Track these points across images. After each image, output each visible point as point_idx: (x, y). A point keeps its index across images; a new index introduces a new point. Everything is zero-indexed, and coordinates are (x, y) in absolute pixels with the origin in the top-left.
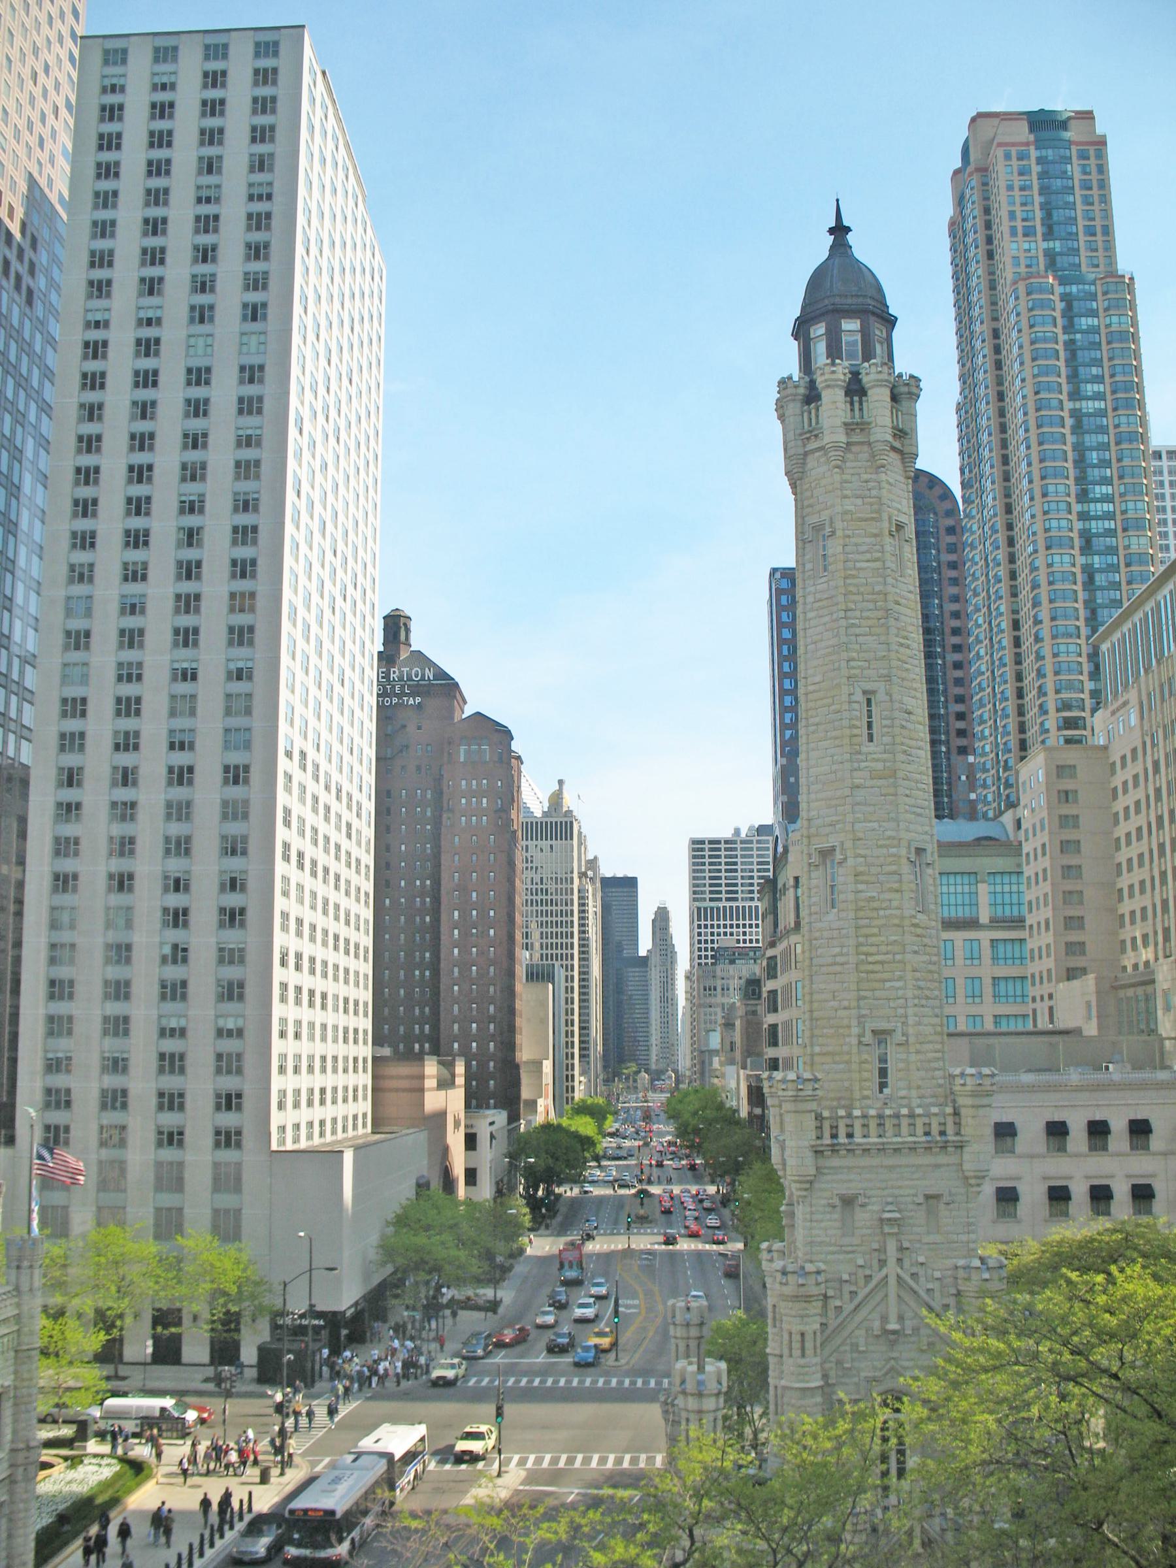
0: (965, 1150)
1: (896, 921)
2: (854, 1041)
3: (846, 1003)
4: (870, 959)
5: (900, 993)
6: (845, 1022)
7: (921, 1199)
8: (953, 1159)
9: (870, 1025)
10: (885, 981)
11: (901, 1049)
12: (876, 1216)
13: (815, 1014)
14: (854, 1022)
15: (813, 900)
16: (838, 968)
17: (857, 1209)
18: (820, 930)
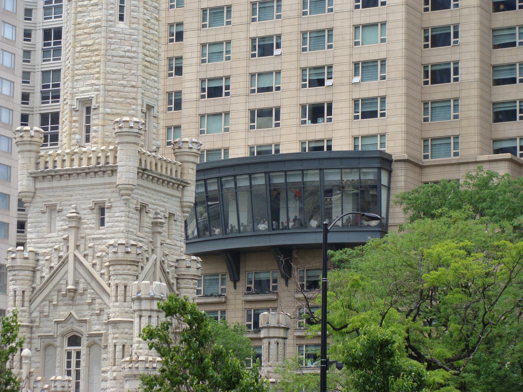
0: (186, 188)
1: (156, 39)
2: (139, 108)
3: (134, 83)
4: (147, 59)
5: (156, 84)
6: (133, 95)
7: (167, 216)
8: (179, 194)
9: (147, 101)
10: (151, 75)
11: (155, 120)
12: (151, 221)
13: (108, 88)
14: (139, 96)
15: (111, 12)
16: (129, 60)
17: (144, 214)
18: (115, 32)
